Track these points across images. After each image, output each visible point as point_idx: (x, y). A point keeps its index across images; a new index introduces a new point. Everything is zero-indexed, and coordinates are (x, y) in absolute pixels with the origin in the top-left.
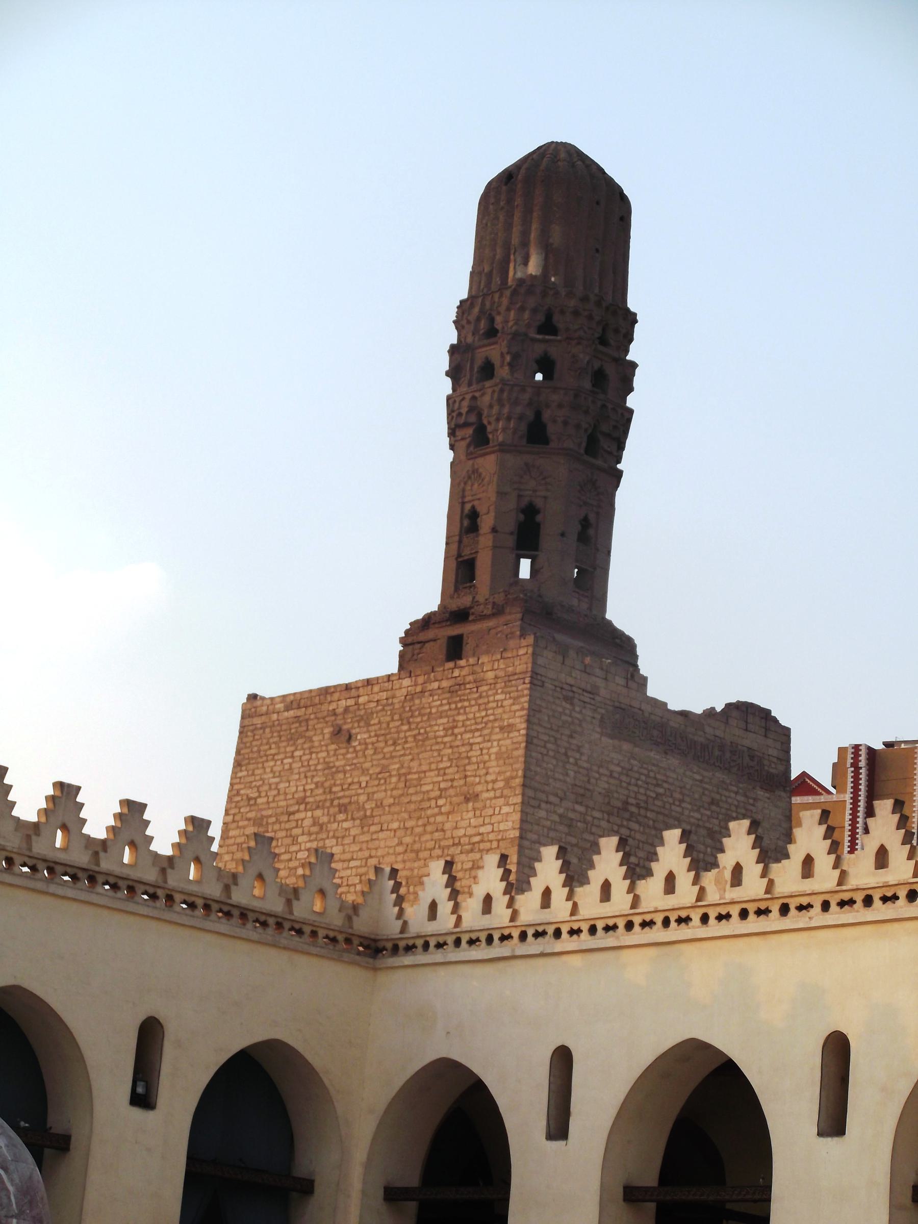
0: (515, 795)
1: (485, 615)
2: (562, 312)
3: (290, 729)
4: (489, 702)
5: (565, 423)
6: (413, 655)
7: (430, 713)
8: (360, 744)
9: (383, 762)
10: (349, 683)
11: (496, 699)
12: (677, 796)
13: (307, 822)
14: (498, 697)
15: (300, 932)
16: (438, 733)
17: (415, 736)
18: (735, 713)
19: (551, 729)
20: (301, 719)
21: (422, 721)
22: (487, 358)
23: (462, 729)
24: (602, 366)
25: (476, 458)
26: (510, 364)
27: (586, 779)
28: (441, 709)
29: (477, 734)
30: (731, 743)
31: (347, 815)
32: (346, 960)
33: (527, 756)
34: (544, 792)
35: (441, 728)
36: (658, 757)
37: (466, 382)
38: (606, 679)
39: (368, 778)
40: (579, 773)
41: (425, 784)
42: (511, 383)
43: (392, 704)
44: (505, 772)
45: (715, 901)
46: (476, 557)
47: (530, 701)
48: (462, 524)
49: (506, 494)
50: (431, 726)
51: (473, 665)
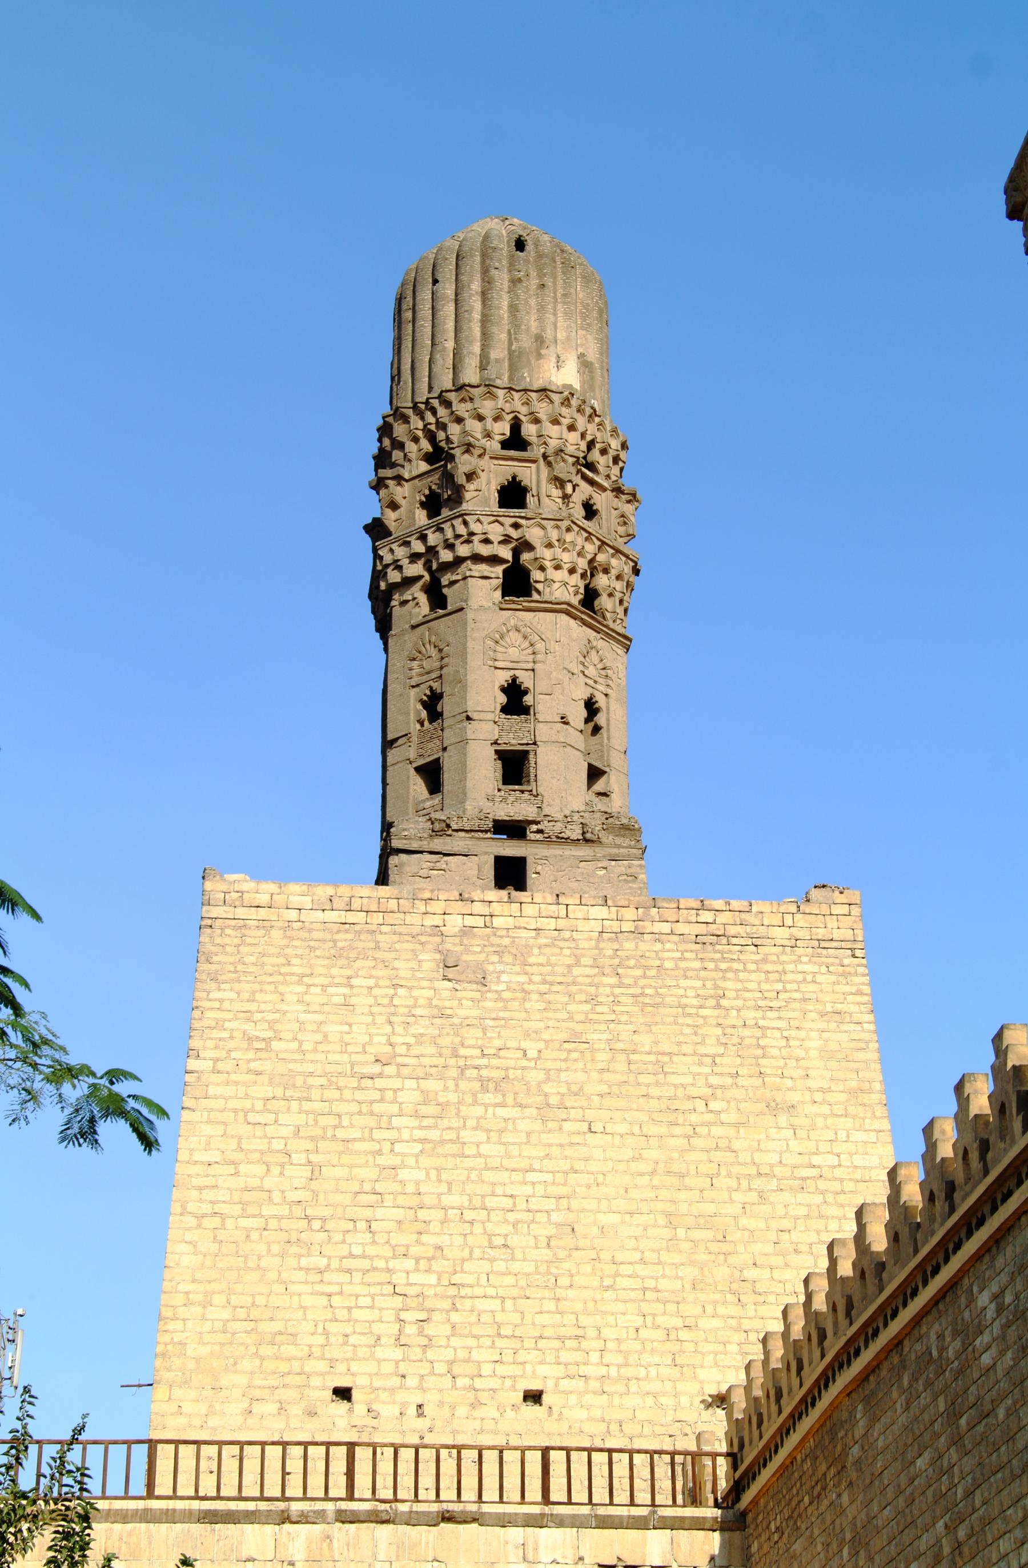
3: (335, 941)
8: (508, 989)
9: (571, 1025)
13: (409, 1096)
14: (800, 967)
17: (634, 996)
20: (357, 928)
21: (644, 976)
29: (769, 1014)
31: (504, 1096)
35: (691, 993)
39: (541, 1045)
41: (674, 1073)
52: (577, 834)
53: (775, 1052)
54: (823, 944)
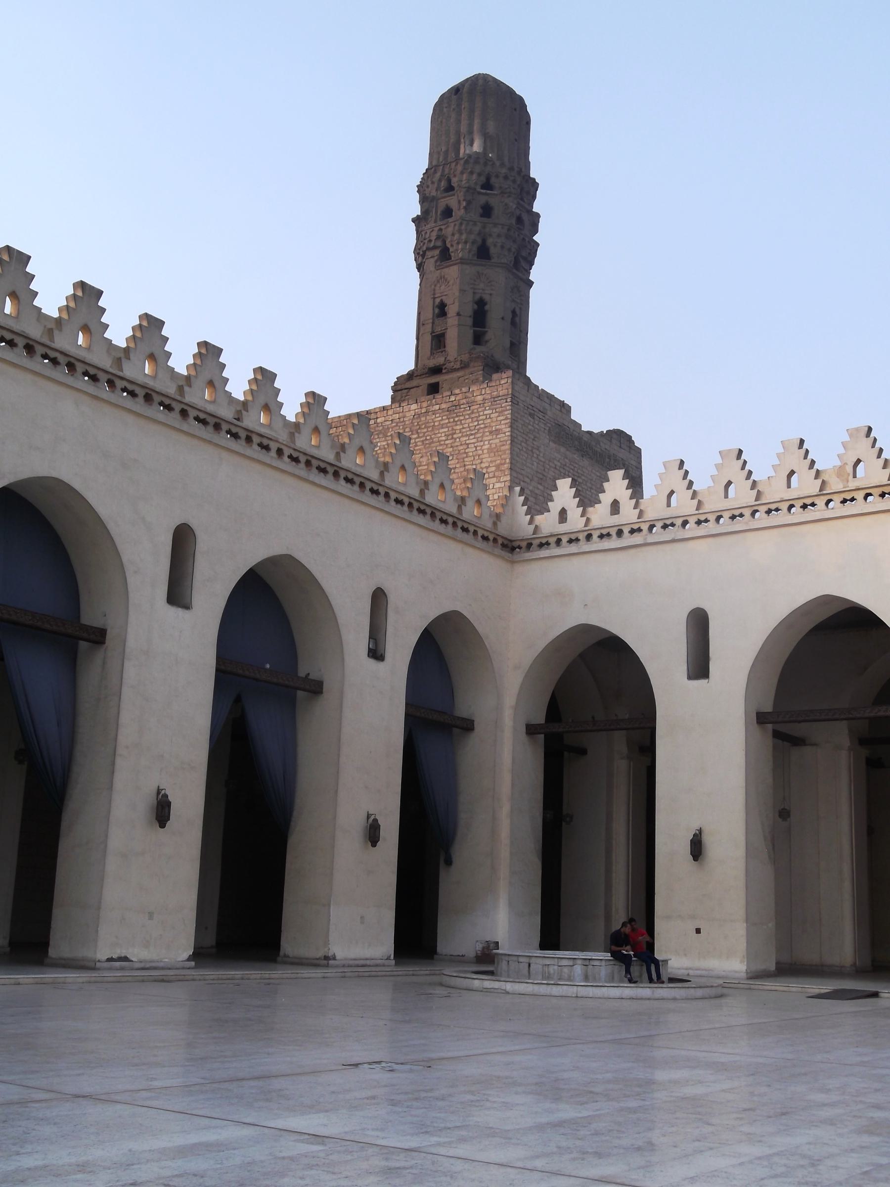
0: (505, 475)
1: (455, 369)
2: (497, 176)
4: (479, 416)
5: (502, 247)
6: (402, 397)
7: (434, 425)
10: (369, 410)
11: (485, 413)
12: (589, 485)
14: (486, 412)
15: (465, 530)
16: (441, 439)
17: (423, 441)
18: (615, 436)
19: (524, 434)
21: (428, 431)
22: (447, 205)
23: (460, 435)
24: (521, 214)
25: (443, 268)
26: (465, 208)
27: (543, 469)
28: (442, 423)
29: (472, 437)
30: (614, 454)
32: (496, 553)
33: (511, 449)
34: (522, 474)
35: (443, 435)
36: (578, 459)
37: (433, 219)
38: (550, 405)
40: (539, 464)
42: (467, 219)
43: (404, 421)
44: (495, 461)
45: (838, 489)
46: (446, 332)
47: (512, 414)
48: (434, 313)
49: (465, 291)
50: (435, 434)
51: (465, 393)
53: (471, 454)
54: (496, 399)
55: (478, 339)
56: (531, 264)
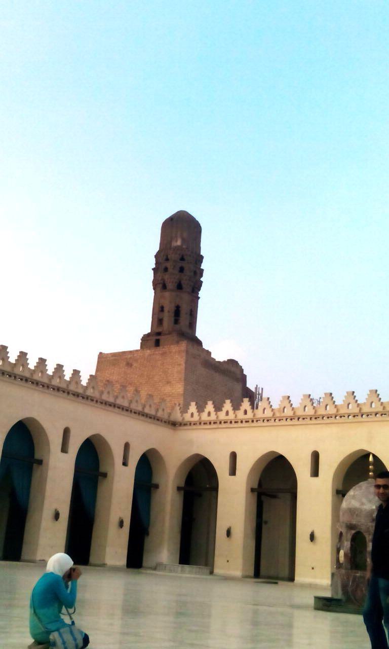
26: (173, 269)
52: (167, 333)
55: (176, 322)
56: (199, 290)
